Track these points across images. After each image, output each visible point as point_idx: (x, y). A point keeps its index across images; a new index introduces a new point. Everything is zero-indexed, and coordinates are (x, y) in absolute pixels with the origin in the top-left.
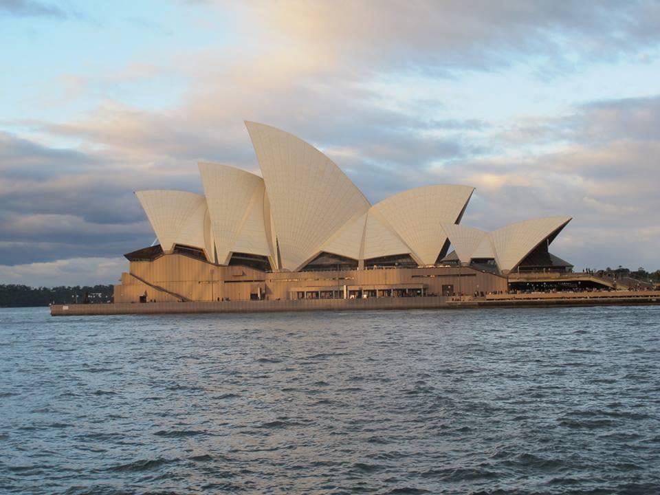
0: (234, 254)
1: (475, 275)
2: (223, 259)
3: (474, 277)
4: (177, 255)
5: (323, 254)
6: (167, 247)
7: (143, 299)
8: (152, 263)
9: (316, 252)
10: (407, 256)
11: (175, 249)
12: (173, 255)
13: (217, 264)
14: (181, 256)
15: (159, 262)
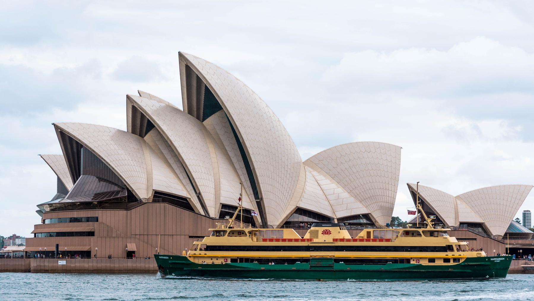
0: (224, 206)
1: (475, 239)
2: (214, 212)
3: (475, 241)
4: (162, 205)
5: (300, 211)
6: (143, 193)
7: (130, 255)
8: (129, 212)
9: (292, 208)
10: (366, 216)
11: (154, 196)
12: (157, 205)
13: (207, 215)
14: (167, 205)
15: (136, 212)
